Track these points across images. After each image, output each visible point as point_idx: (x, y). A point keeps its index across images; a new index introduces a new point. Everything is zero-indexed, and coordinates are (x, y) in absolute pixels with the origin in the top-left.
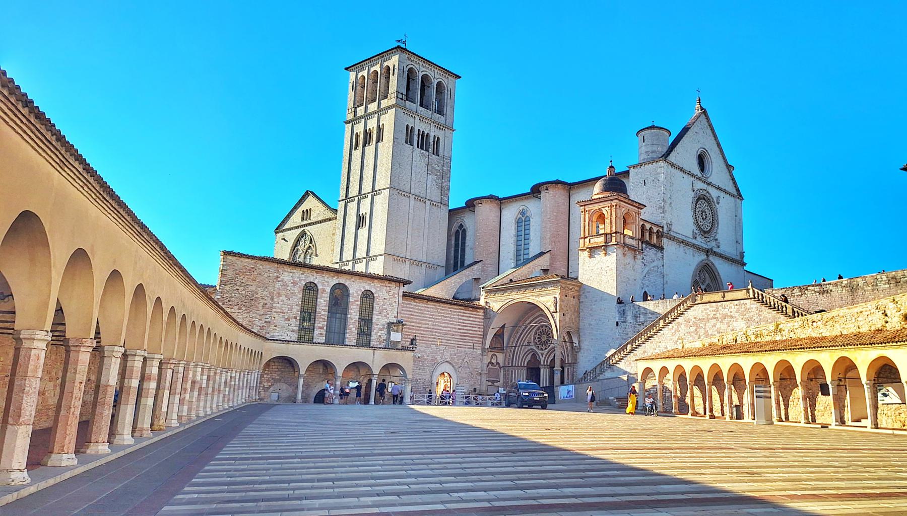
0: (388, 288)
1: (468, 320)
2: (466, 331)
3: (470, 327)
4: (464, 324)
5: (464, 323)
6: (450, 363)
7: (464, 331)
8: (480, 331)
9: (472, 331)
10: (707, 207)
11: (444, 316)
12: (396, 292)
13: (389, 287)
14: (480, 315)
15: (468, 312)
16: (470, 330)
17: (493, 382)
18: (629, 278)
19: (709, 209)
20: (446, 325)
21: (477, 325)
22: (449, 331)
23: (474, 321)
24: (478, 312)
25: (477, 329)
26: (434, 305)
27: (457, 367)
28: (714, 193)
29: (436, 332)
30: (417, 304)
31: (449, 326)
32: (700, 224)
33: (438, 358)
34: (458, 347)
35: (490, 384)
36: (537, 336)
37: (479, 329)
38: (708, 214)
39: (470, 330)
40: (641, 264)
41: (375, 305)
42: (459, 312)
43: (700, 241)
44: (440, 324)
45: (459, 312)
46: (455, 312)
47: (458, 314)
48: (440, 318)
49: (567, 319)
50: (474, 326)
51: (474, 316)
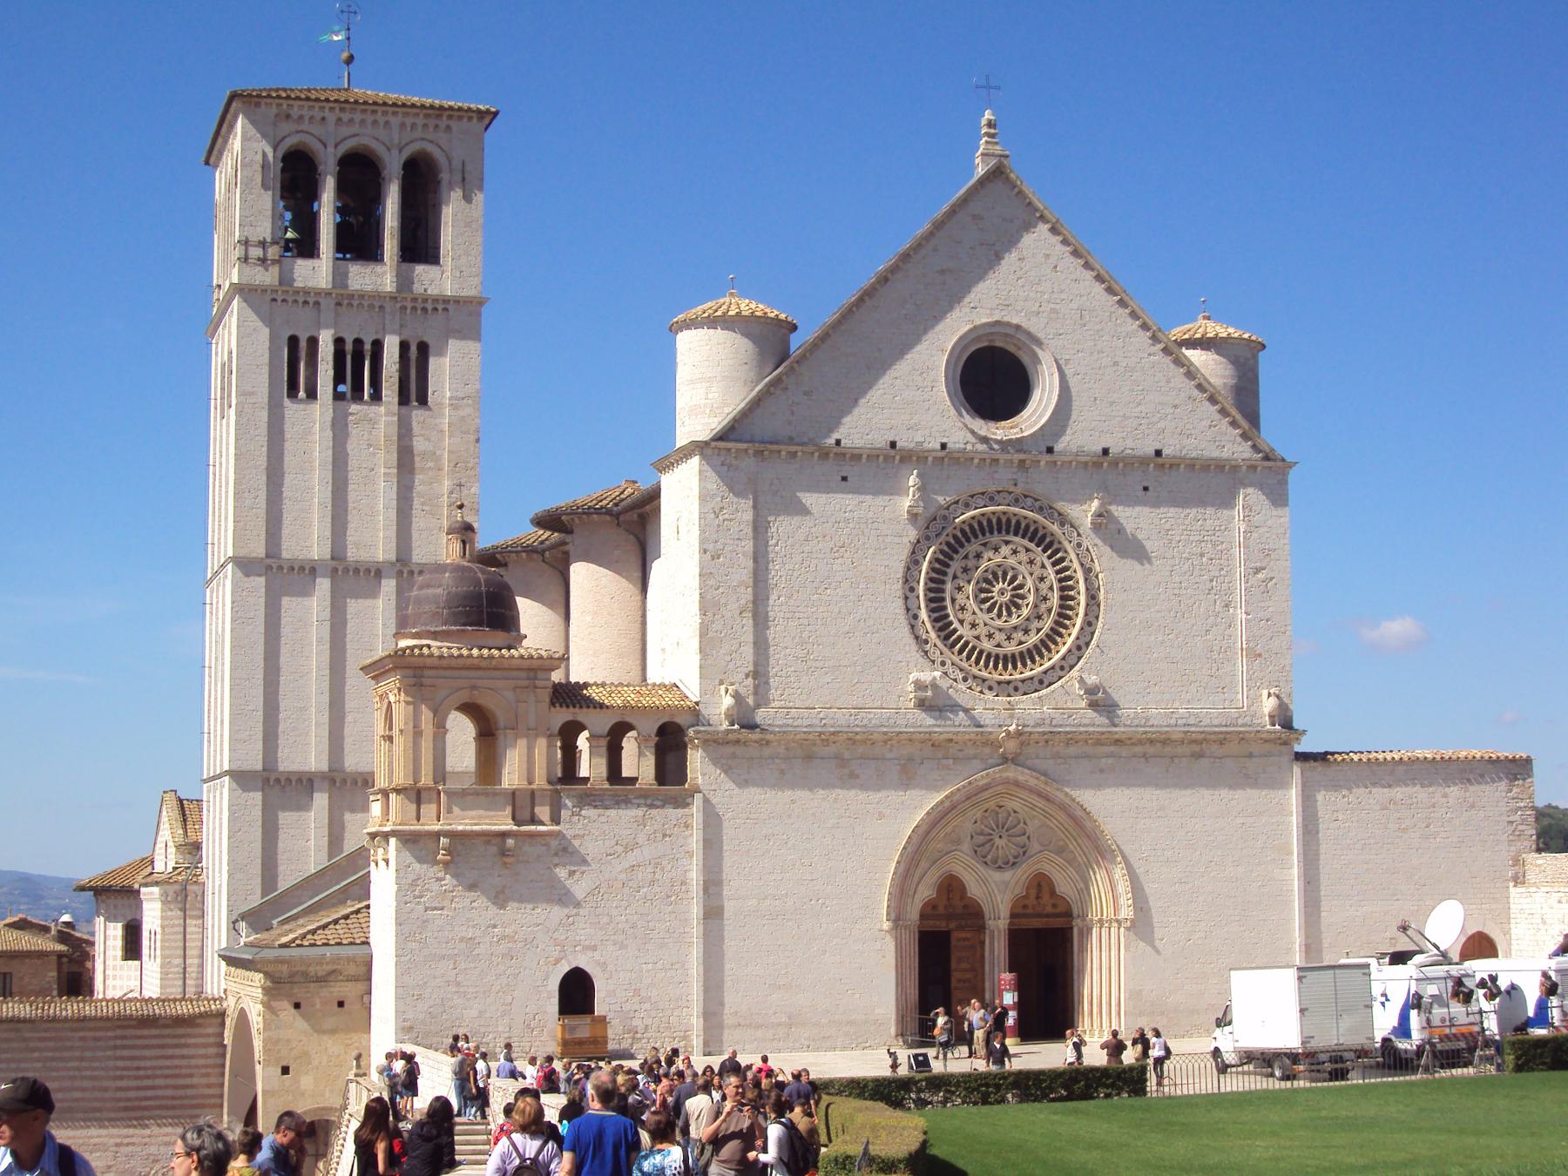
1: (157, 1058)
2: (149, 1093)
3: (167, 1077)
4: (141, 1073)
5: (138, 1068)
7: (142, 1093)
9: (176, 1087)
10: (1023, 556)
11: (53, 1059)
14: (209, 1035)
16: (167, 1087)
20: (67, 1084)
21: (197, 1067)
22: (77, 1100)
23: (183, 1057)
24: (198, 1025)
25: (195, 1081)
26: (11, 1030)
31: (77, 1084)
34: (117, 1145)
37: (204, 1081)
38: (1030, 583)
39: (167, 1087)
42: (116, 1038)
45: (116, 1038)
46: (96, 1039)
47: (112, 1043)
48: (39, 1065)
49: (306, 1082)
50: (188, 1071)
51: (183, 1041)
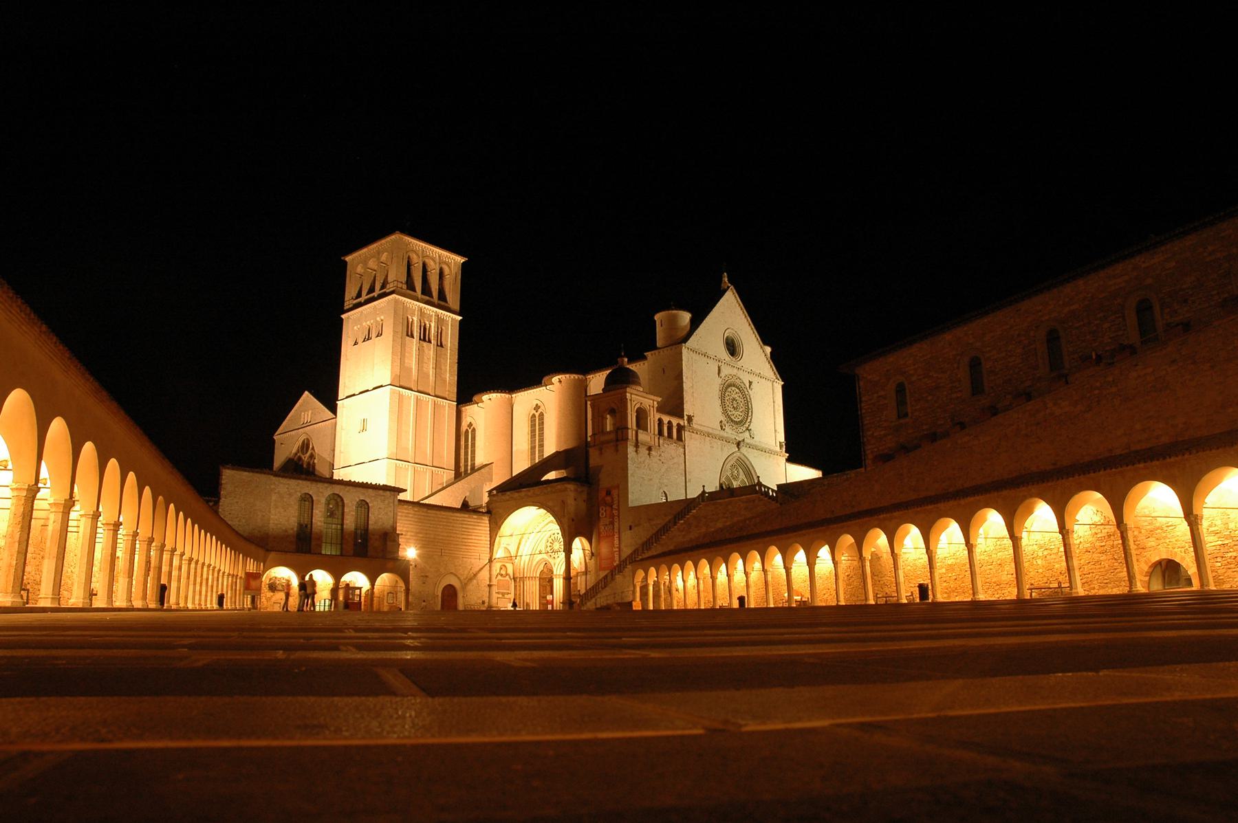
0: (383, 497)
6: (456, 575)
8: (486, 540)
11: (446, 526)
12: (392, 501)
13: (384, 496)
15: (473, 520)
17: (503, 594)
18: (643, 478)
19: (741, 396)
27: (462, 578)
28: (746, 378)
29: (438, 542)
30: (417, 513)
32: (730, 413)
33: (442, 570)
35: (500, 596)
36: (549, 544)
37: (485, 539)
40: (658, 461)
41: (370, 515)
43: (729, 432)
44: (442, 534)
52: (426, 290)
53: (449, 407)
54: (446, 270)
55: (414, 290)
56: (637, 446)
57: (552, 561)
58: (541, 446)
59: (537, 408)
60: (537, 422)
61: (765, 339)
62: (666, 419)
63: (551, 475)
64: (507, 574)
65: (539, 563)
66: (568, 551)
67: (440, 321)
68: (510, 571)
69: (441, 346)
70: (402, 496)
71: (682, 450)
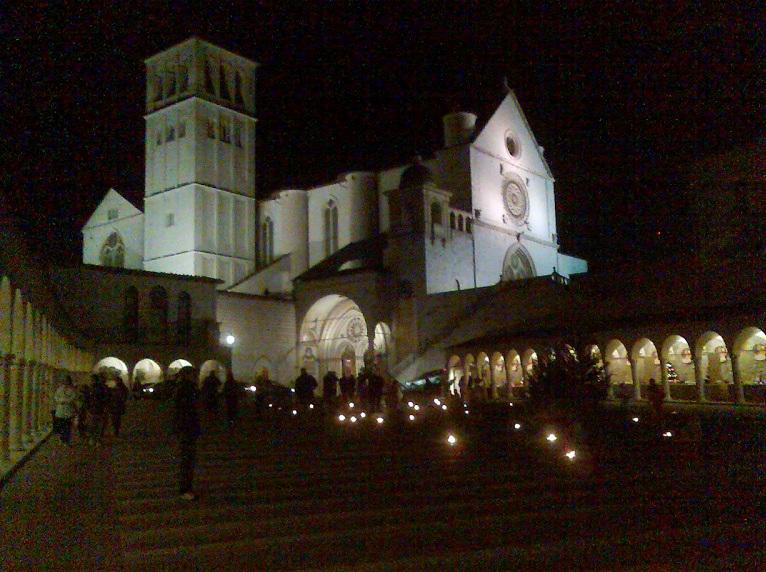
52: (225, 93)
53: (248, 203)
54: (242, 74)
55: (213, 93)
56: (433, 238)
57: (353, 344)
58: (336, 237)
59: (331, 202)
60: (331, 215)
61: (540, 141)
62: (457, 213)
63: (346, 266)
64: (312, 356)
65: (342, 345)
66: (371, 334)
67: (239, 124)
68: (315, 353)
69: (240, 146)
70: (220, 287)
71: (470, 242)
